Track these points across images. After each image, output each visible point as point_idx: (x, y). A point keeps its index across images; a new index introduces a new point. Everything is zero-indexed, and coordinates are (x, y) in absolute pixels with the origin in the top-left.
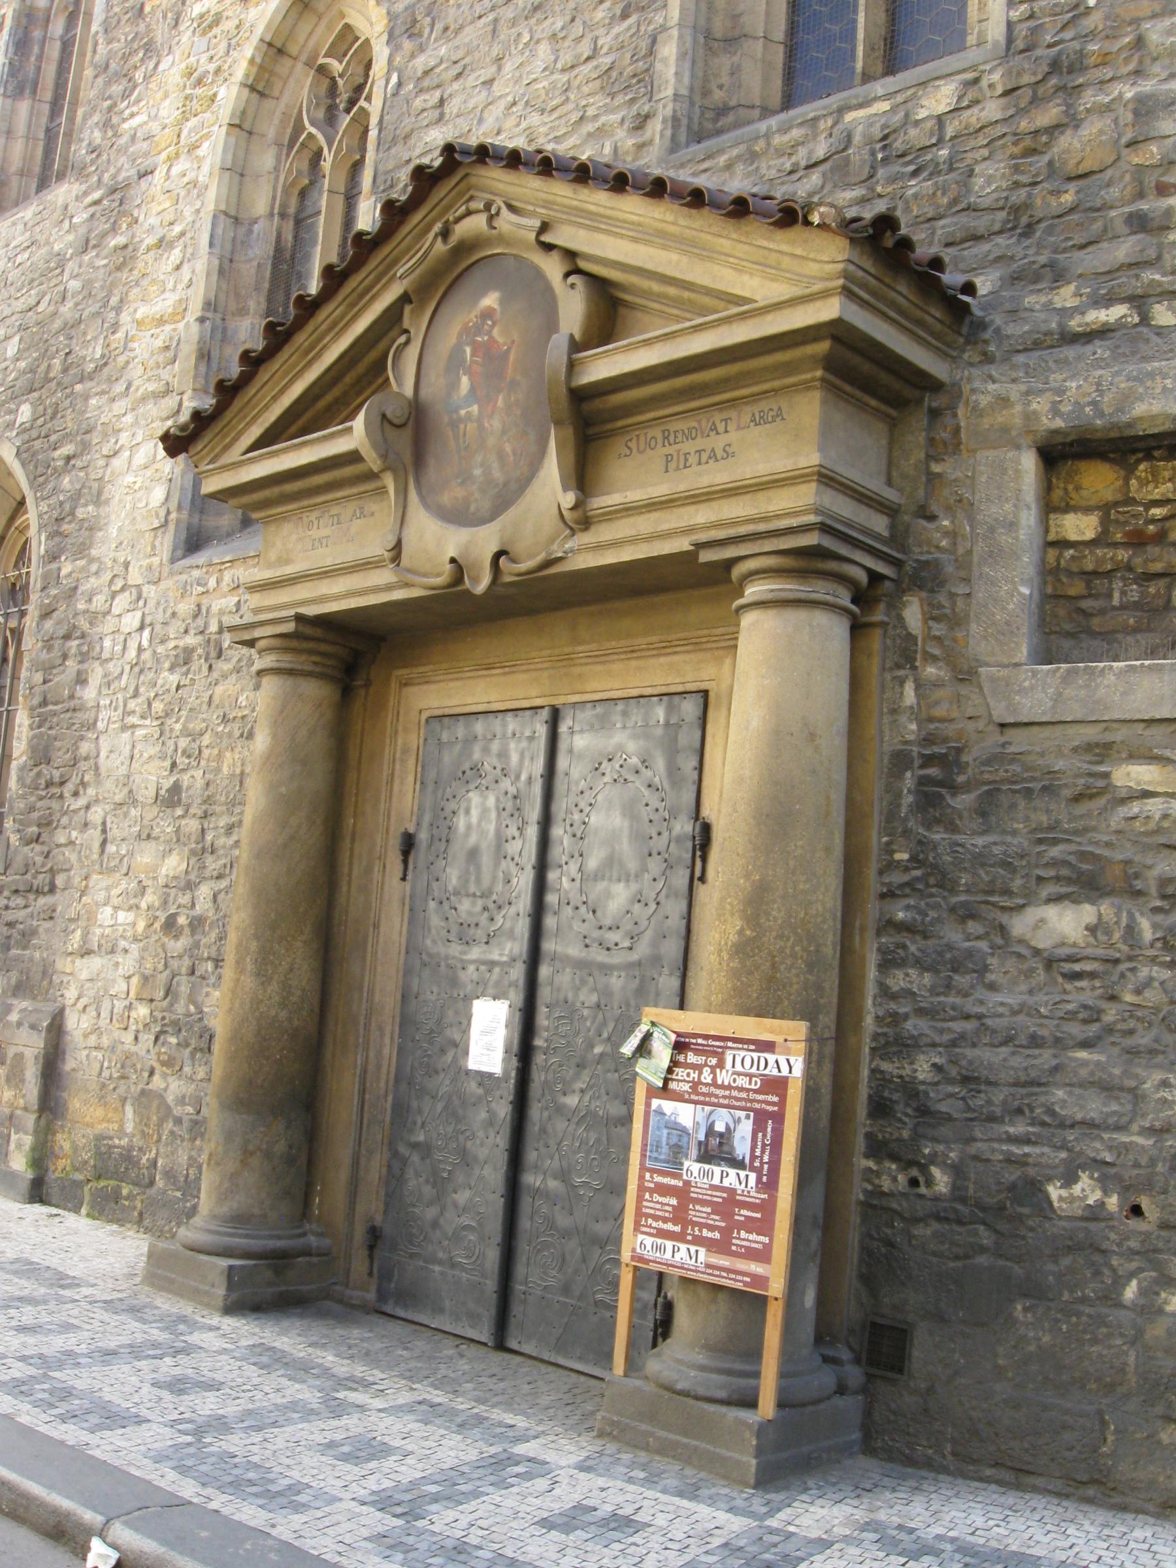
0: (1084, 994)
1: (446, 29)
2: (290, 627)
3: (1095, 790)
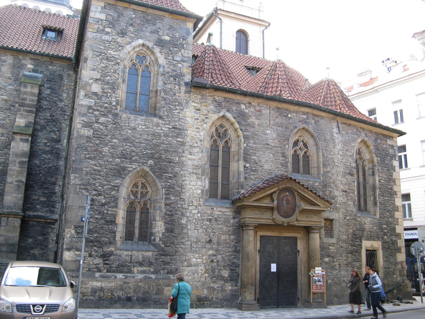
0: (328, 265)
3: (329, 249)
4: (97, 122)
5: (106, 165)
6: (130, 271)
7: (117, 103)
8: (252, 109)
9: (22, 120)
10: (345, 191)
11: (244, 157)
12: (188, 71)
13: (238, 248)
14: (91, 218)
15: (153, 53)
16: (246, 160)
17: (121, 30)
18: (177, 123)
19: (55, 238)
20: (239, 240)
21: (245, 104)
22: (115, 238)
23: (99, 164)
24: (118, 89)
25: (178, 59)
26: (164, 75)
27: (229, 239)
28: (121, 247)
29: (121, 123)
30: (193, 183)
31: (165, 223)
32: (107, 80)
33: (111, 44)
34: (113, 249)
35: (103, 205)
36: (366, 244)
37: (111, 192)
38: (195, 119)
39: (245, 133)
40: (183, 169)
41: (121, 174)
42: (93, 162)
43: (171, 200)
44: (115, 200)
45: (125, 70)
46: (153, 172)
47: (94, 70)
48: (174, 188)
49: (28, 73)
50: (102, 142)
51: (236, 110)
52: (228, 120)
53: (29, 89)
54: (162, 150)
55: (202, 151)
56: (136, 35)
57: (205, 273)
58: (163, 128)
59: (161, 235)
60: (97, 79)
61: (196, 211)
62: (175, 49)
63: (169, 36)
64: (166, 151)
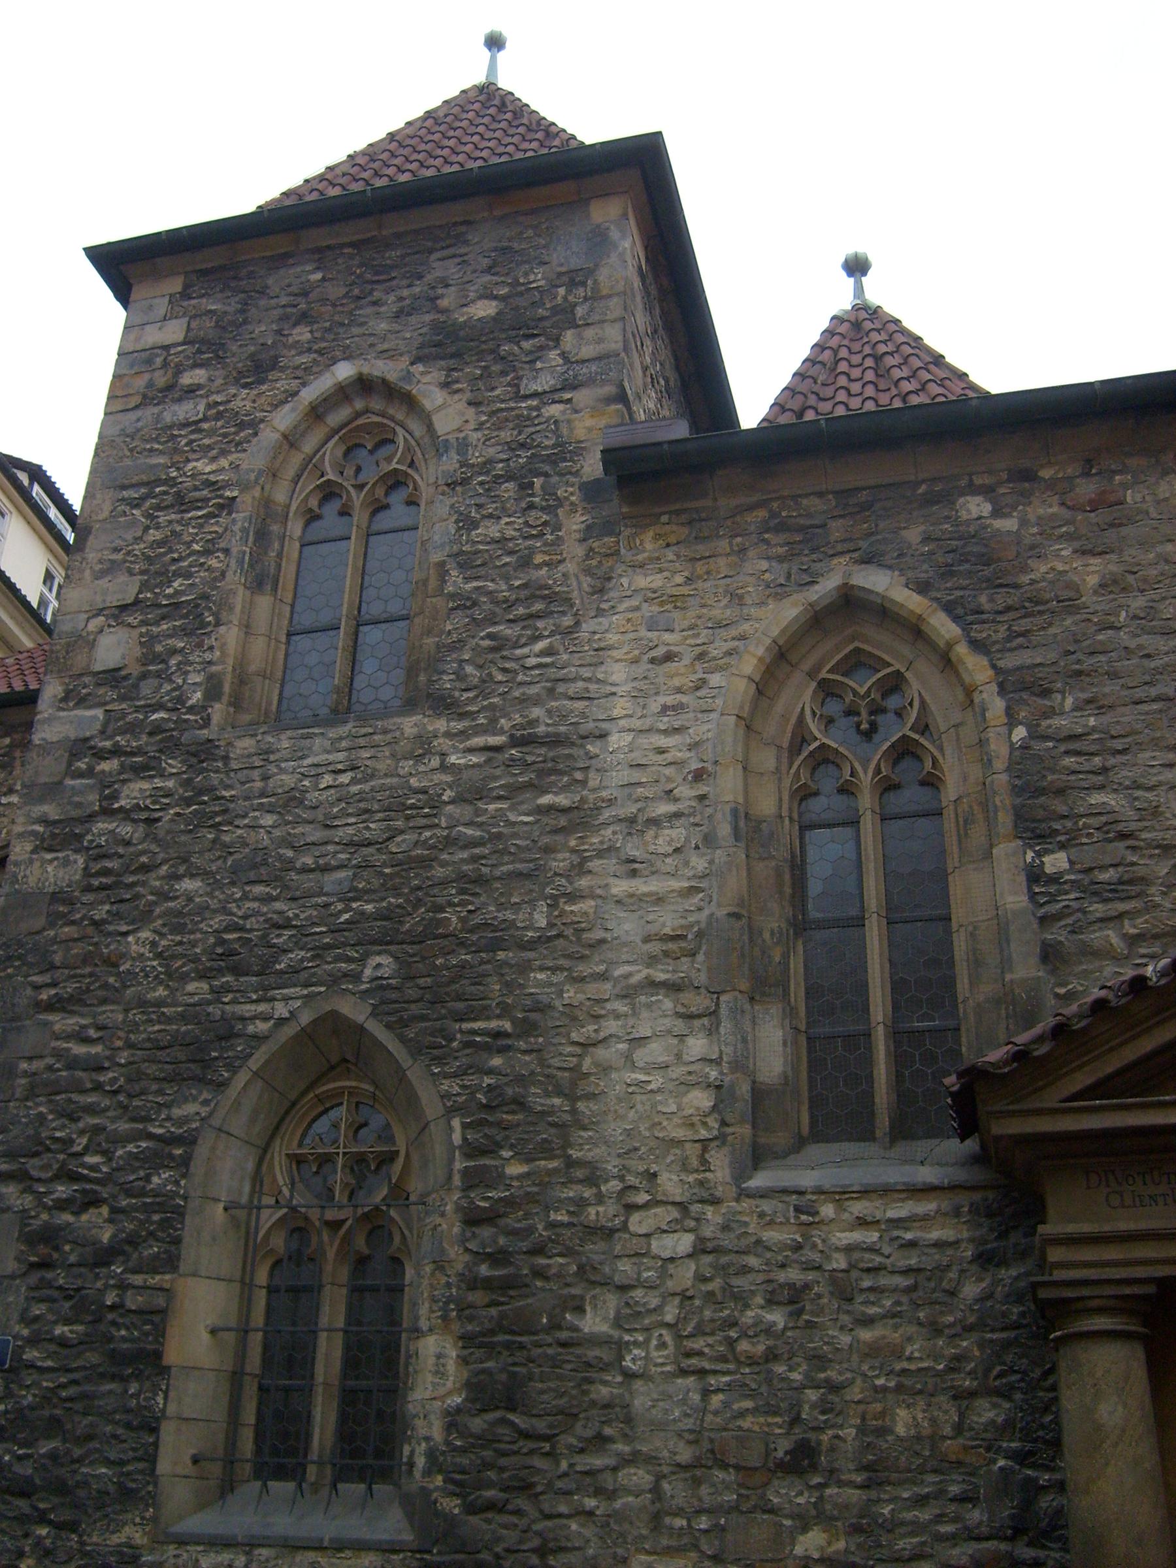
1: (1089, 701)
2: (1151, 1289)
4: (108, 812)
5: (135, 1027)
7: (213, 692)
8: (1046, 507)
11: (1020, 816)
12: (603, 422)
13: (1046, 1502)
14: (34, 1341)
16: (1036, 831)
17: (252, 356)
18: (536, 712)
20: (1040, 1439)
21: (987, 491)
22: (151, 1459)
23: (100, 1028)
24: (218, 624)
26: (464, 482)
27: (959, 1429)
28: (195, 1524)
29: (228, 787)
30: (655, 1051)
31: (467, 1340)
32: (169, 596)
33: (200, 431)
34: (139, 1538)
35: (104, 1257)
37: (147, 1178)
38: (652, 661)
39: (1008, 662)
40: (583, 969)
41: (206, 1064)
43: (496, 1178)
44: (165, 1224)
45: (275, 528)
46: (388, 1026)
48: (520, 1104)
50: (123, 907)
51: (927, 539)
52: (884, 613)
54: (444, 883)
55: (709, 840)
56: (318, 352)
58: (453, 759)
59: (437, 1432)
60: (123, 608)
61: (684, 1242)
62: (527, 345)
63: (495, 298)
64: (472, 883)
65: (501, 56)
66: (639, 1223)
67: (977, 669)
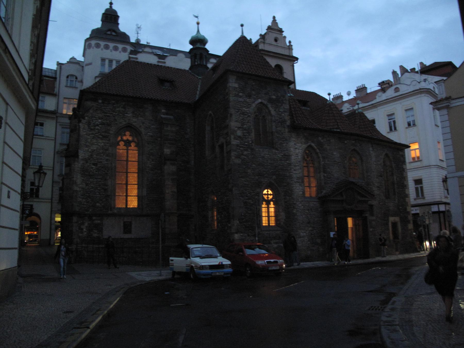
4: (243, 155)
6: (270, 243)
7: (252, 142)
9: (168, 150)
10: (378, 187)
15: (267, 107)
16: (324, 172)
19: (194, 228)
25: (281, 110)
30: (298, 188)
36: (392, 219)
42: (243, 179)
47: (236, 121)
49: (163, 116)
53: (169, 128)
57: (309, 241)
61: (301, 205)
65: (243, 27)
66: (298, 203)
67: (320, 155)
